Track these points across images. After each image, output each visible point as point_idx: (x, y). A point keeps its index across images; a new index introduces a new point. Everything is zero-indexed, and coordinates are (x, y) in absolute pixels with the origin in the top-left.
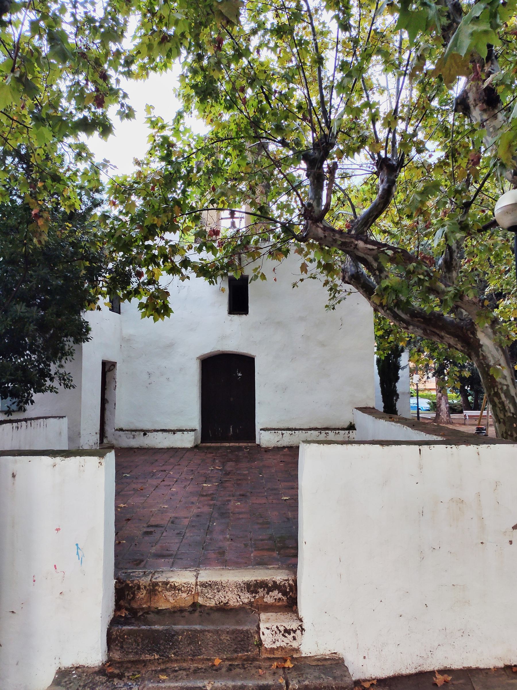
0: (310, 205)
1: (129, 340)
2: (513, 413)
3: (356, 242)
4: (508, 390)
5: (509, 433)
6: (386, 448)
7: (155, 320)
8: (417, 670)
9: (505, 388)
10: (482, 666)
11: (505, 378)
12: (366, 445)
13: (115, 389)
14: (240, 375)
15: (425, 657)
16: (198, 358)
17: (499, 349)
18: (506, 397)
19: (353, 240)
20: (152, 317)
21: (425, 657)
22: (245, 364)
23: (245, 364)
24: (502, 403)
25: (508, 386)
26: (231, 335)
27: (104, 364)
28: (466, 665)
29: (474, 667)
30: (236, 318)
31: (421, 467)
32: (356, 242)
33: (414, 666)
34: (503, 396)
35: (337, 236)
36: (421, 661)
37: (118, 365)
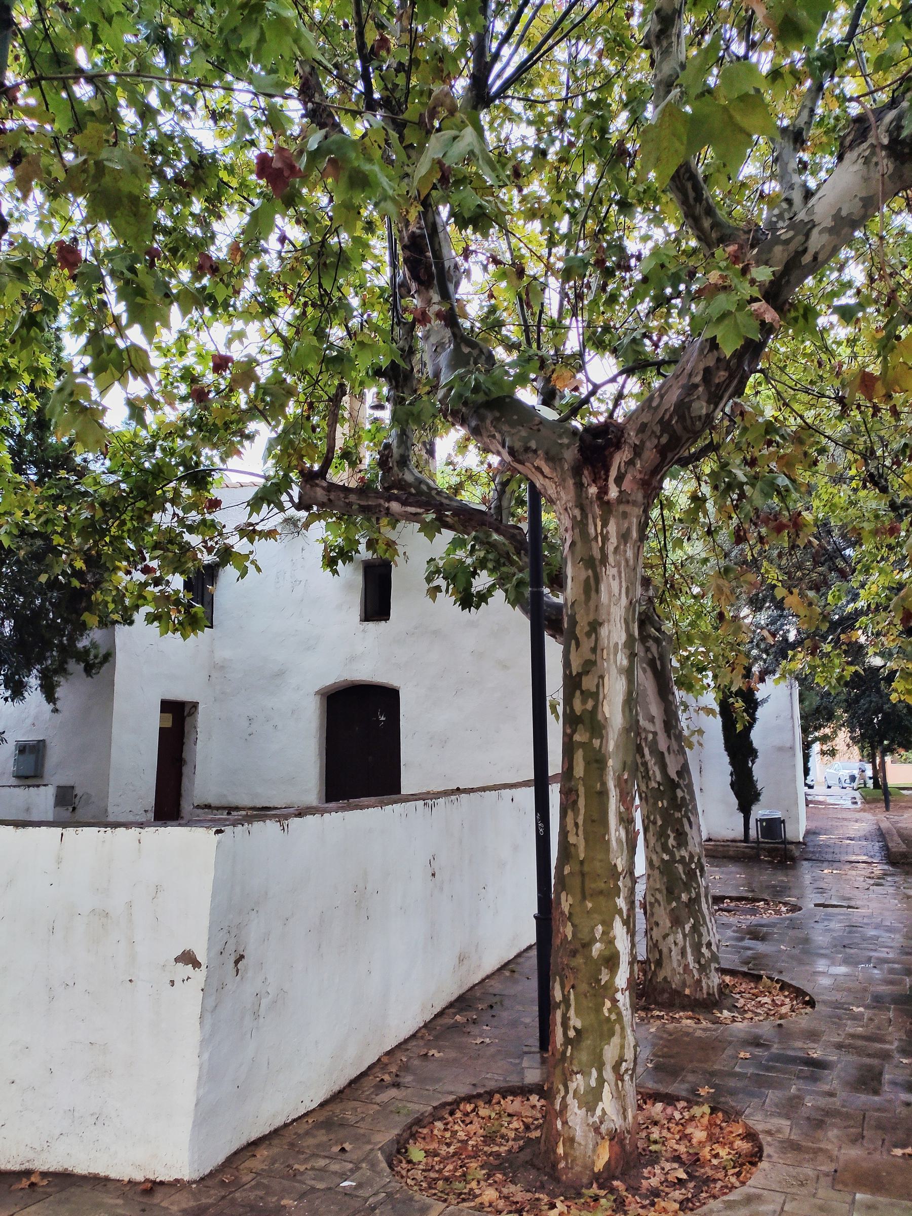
0: (621, 430)
1: (222, 667)
2: (659, 784)
3: (387, 505)
4: (655, 741)
5: (652, 818)
6: (21, 831)
7: (185, 637)
8: (23, 1168)
9: (650, 737)
10: (113, 1176)
11: (652, 720)
12: (43, 828)
13: (195, 743)
14: (383, 718)
15: (39, 1149)
16: (317, 693)
17: (648, 669)
18: (651, 753)
19: (382, 501)
20: (178, 634)
21: (39, 1149)
22: (383, 699)
23: (383, 699)
24: (645, 764)
25: (655, 734)
26: (365, 653)
27: (167, 706)
28: (92, 1170)
29: (102, 1174)
30: (371, 625)
31: (59, 861)
32: (387, 505)
33: (19, 1160)
34: (646, 751)
35: (353, 498)
36: (31, 1155)
37: (201, 708)
